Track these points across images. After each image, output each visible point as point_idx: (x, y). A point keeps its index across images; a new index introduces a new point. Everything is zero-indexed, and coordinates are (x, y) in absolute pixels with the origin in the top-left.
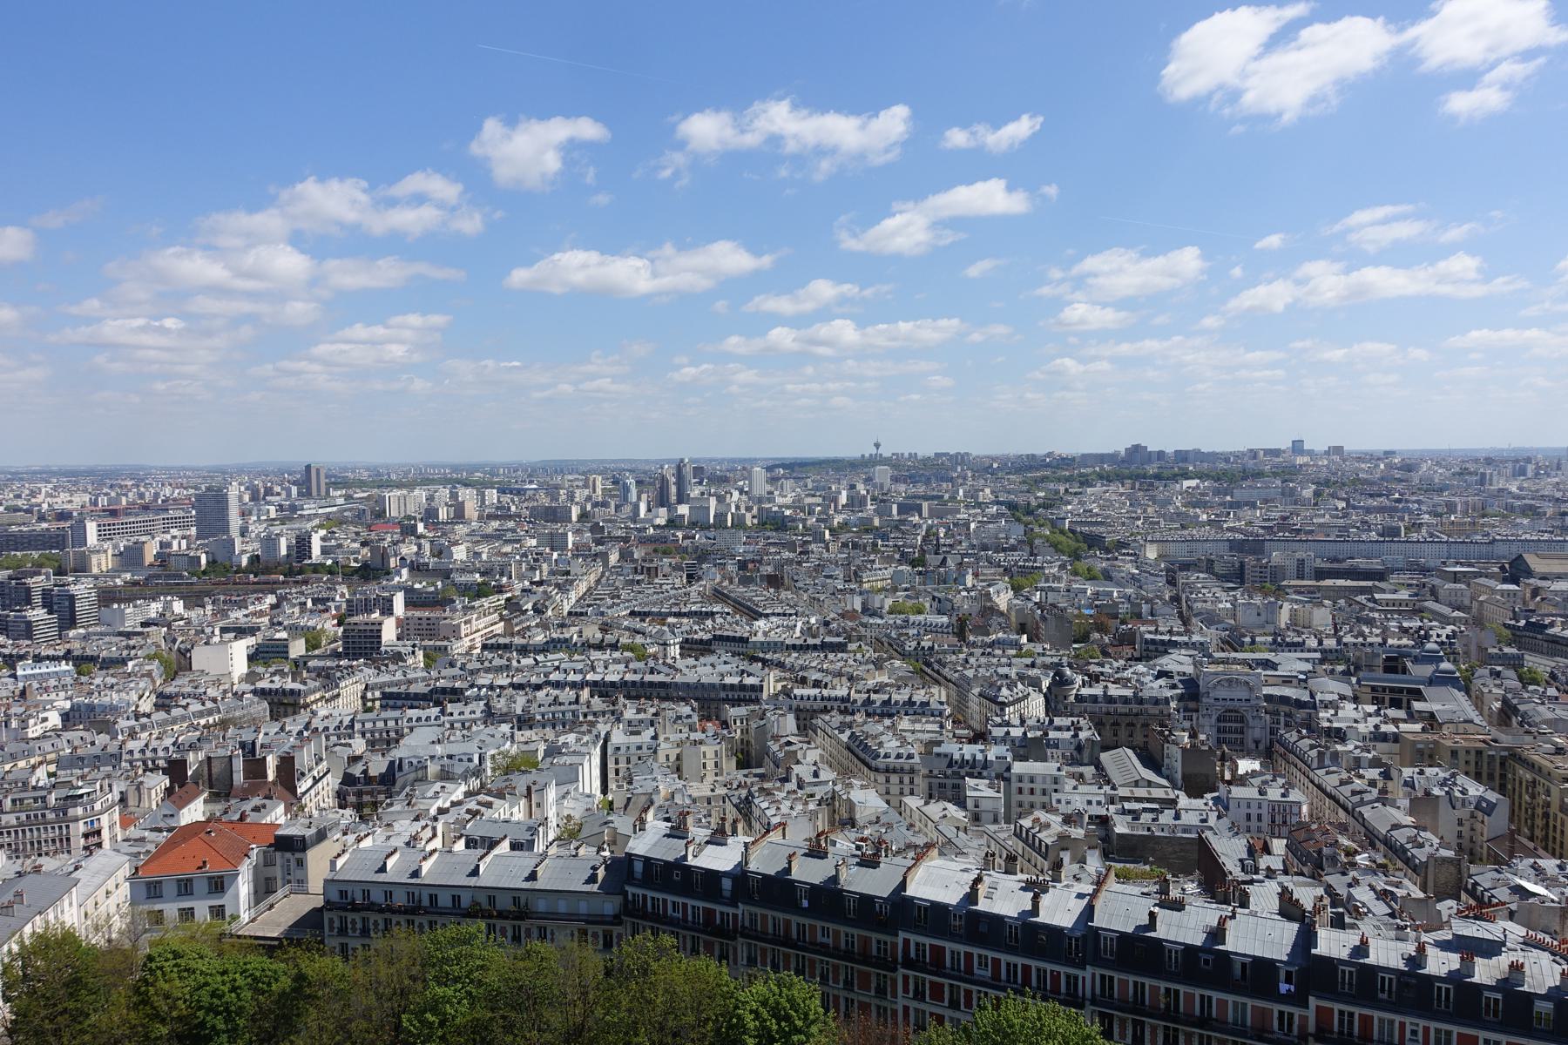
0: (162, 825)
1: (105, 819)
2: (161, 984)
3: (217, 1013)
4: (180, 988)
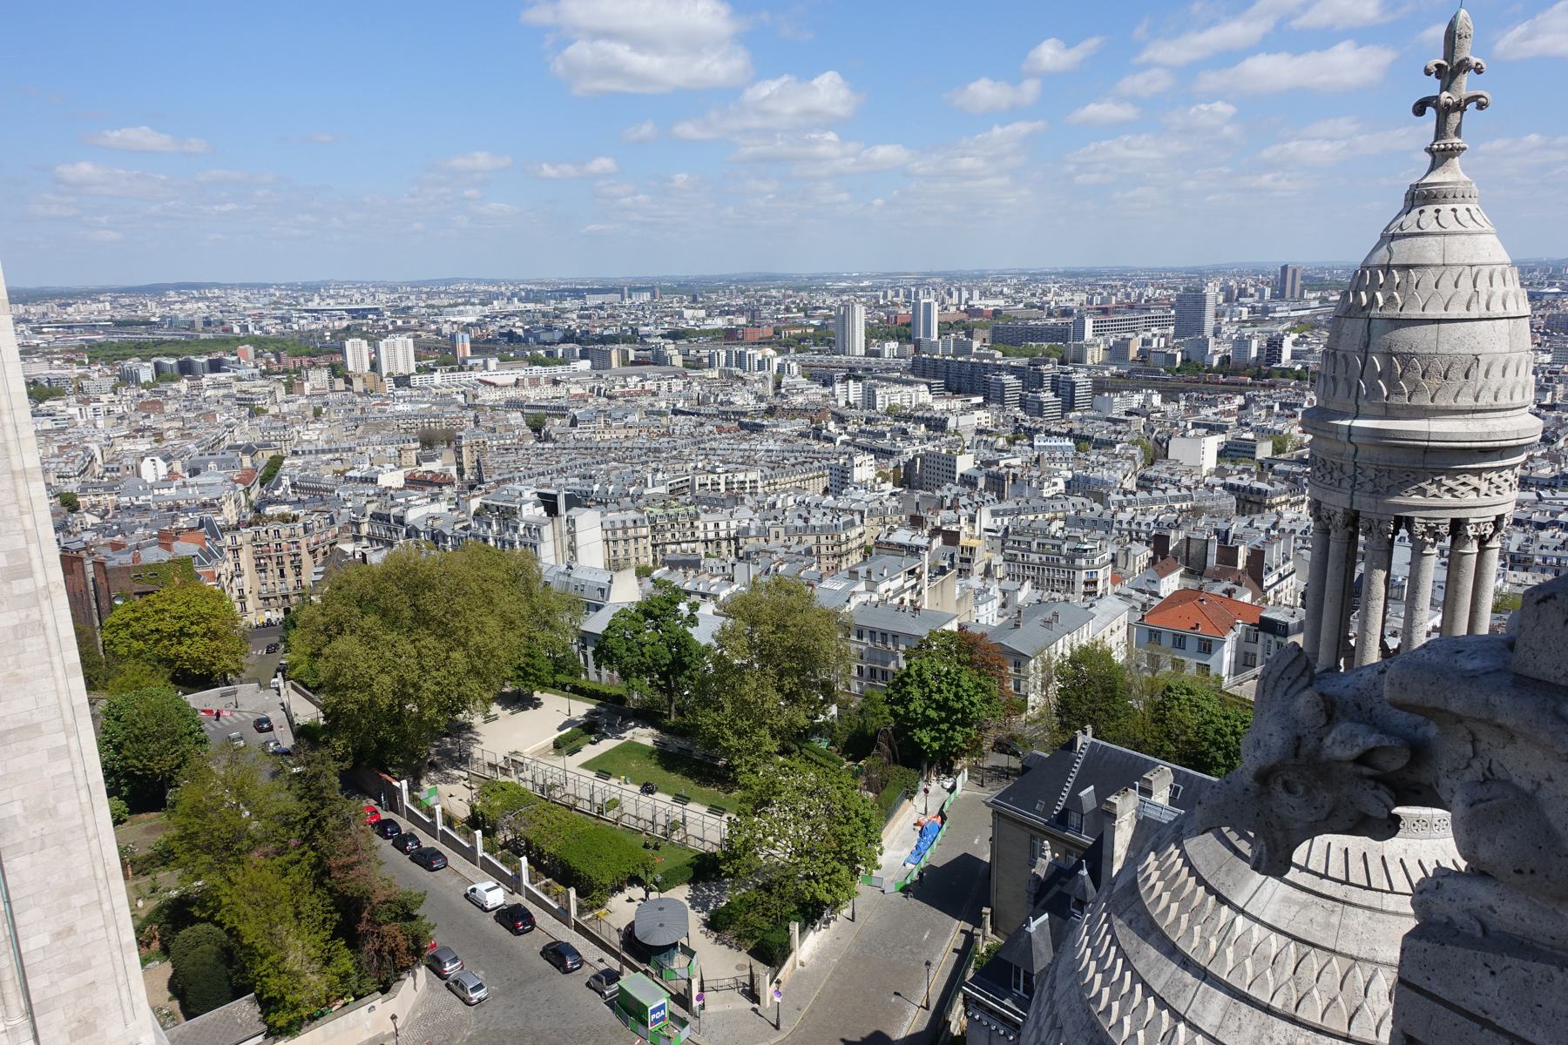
0: (1145, 588)
1: (1101, 572)
2: (1176, 711)
3: (1219, 749)
4: (1192, 720)
